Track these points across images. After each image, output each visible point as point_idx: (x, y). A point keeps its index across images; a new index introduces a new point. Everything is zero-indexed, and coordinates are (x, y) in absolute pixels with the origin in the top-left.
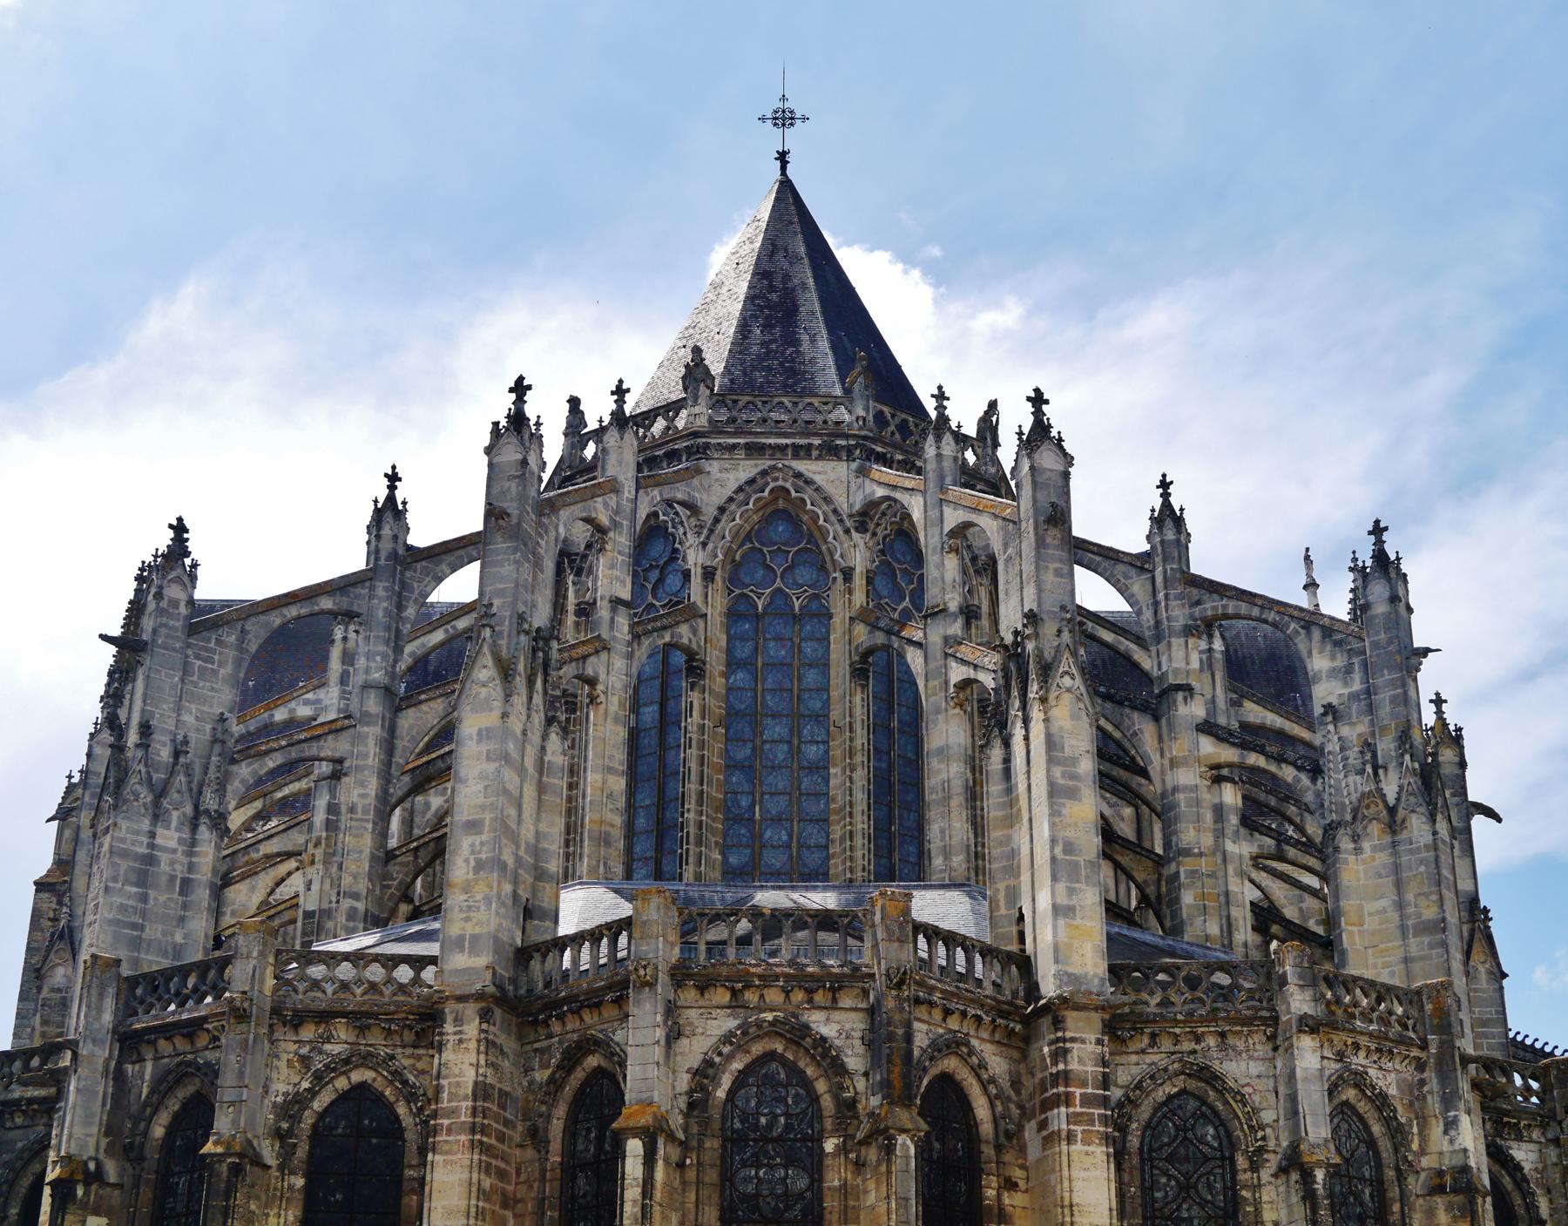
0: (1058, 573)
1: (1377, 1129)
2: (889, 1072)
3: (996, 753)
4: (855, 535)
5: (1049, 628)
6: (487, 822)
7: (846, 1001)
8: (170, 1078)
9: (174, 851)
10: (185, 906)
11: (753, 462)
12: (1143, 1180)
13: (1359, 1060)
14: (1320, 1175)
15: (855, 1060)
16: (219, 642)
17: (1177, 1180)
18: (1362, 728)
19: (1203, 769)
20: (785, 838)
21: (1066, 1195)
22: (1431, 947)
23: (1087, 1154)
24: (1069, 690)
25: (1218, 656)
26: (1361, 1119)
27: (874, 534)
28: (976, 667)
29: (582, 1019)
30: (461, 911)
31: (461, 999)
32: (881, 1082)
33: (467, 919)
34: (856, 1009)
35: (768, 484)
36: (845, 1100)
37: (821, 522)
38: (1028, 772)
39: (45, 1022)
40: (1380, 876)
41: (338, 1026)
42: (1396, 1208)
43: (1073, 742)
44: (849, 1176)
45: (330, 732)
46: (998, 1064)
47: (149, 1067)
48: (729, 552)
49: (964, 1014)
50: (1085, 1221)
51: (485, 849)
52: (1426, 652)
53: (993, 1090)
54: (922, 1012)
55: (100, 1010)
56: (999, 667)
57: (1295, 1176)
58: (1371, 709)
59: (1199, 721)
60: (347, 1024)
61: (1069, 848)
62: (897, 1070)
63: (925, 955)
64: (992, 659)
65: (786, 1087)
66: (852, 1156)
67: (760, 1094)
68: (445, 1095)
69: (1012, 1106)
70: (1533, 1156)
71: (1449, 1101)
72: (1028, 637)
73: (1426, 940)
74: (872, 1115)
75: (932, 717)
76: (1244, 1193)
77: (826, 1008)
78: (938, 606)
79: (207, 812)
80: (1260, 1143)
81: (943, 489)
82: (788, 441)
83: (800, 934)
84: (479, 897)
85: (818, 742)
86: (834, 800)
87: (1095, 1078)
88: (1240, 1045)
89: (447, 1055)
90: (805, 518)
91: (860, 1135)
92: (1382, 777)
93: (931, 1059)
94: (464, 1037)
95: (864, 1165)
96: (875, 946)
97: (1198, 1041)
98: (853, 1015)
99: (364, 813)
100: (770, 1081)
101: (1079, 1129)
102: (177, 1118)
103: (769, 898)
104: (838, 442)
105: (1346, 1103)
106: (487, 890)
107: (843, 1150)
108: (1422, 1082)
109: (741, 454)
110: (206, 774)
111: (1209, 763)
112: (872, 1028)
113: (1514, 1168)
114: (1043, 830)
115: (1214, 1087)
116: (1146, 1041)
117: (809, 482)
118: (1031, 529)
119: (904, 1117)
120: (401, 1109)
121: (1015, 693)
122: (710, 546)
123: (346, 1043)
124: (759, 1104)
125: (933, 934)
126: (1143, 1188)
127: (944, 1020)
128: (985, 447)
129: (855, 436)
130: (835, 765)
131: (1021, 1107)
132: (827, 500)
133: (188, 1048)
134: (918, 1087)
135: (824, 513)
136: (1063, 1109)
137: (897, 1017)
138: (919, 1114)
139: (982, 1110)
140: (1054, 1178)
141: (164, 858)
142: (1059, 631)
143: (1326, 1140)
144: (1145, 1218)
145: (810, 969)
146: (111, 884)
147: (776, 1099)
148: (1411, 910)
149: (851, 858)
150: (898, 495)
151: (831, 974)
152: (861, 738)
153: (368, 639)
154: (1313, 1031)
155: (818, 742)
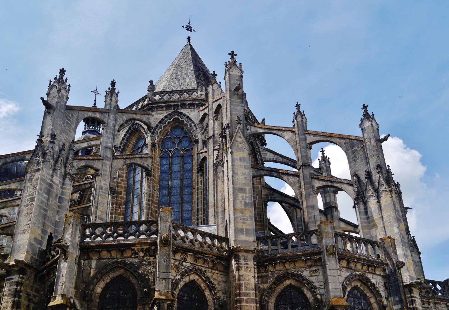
8: (108, 268)
9: (58, 185)
10: (60, 207)
16: (72, 115)
29: (284, 266)
30: (241, 219)
31: (247, 251)
33: (244, 223)
34: (380, 275)
41: (189, 256)
45: (97, 159)
47: (94, 263)
51: (247, 199)
55: (75, 236)
60: (192, 256)
67: (354, 301)
68: (243, 287)
77: (372, 273)
78: (307, 163)
79: (69, 174)
89: (242, 272)
94: (249, 266)
97: (429, 305)
99: (105, 190)
100: (355, 296)
102: (107, 285)
106: (250, 214)
110: (68, 160)
111: (344, 230)
120: (207, 293)
122: (204, 134)
123: (191, 263)
124: (354, 304)
133: (119, 256)
141: (55, 186)
146: (40, 191)
153: (107, 132)
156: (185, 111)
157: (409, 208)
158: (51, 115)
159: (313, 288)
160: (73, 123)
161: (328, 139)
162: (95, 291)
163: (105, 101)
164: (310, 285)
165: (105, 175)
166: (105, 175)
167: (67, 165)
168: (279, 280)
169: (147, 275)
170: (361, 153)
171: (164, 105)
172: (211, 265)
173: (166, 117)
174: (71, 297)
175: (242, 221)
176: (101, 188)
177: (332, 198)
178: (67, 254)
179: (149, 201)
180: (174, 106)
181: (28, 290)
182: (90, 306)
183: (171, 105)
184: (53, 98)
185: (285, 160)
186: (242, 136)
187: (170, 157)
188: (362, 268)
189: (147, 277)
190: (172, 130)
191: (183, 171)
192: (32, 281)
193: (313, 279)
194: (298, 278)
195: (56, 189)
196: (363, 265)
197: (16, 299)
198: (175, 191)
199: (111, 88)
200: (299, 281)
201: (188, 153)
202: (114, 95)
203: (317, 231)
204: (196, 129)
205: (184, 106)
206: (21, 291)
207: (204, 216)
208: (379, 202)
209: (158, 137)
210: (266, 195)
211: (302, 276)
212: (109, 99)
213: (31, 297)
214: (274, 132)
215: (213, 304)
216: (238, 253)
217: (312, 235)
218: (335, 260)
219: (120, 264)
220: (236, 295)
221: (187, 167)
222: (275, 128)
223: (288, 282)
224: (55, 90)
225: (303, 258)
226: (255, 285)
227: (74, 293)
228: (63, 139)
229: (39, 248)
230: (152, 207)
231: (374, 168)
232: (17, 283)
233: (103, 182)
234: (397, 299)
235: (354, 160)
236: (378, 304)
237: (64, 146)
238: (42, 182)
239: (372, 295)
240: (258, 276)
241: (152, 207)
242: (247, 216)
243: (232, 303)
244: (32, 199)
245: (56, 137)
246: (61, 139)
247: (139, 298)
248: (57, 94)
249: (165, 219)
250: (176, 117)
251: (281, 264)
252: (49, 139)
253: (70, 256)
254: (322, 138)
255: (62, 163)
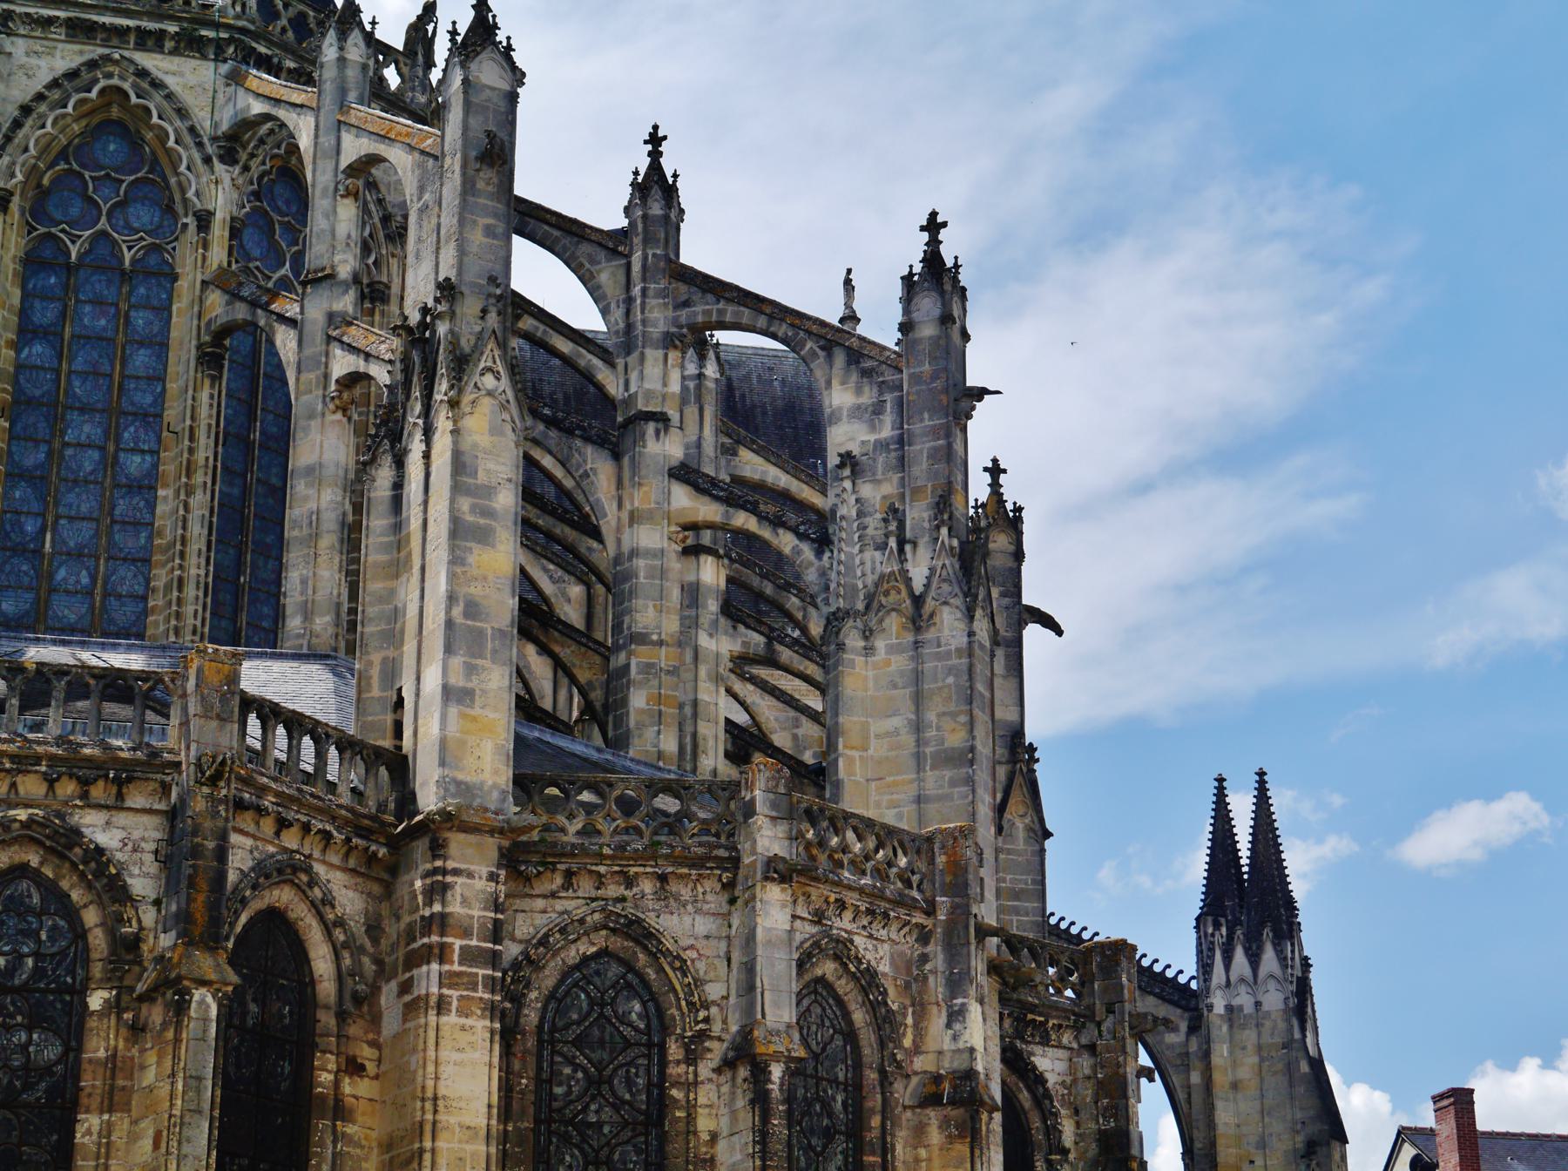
0: (489, 231)
1: (859, 1017)
2: (190, 900)
3: (384, 475)
4: (219, 167)
5: (470, 307)
7: (136, 799)
11: (77, 47)
12: (539, 1068)
13: (843, 924)
14: (777, 1071)
15: (142, 882)
17: (585, 1071)
18: (889, 488)
19: (674, 528)
20: (85, 580)
21: (430, 1083)
22: (953, 783)
23: (463, 1028)
24: (490, 394)
25: (711, 385)
26: (840, 1002)
27: (246, 168)
28: (368, 356)
32: (177, 915)
34: (150, 811)
35: (96, 81)
36: (124, 937)
37: (171, 143)
38: (426, 503)
40: (895, 687)
42: (876, 1121)
43: (491, 466)
44: (121, 1044)
46: (349, 900)
48: (33, 172)
49: (306, 828)
50: (452, 1120)
52: (981, 393)
53: (340, 936)
54: (246, 821)
56: (397, 357)
57: (743, 1072)
58: (902, 464)
59: (674, 463)
61: (472, 609)
62: (201, 898)
63: (258, 746)
64: (389, 346)
65: (39, 915)
66: (128, 1016)
69: (366, 960)
70: (1061, 1066)
71: (956, 984)
72: (440, 316)
73: (948, 774)
74: (160, 959)
75: (302, 423)
76: (674, 1092)
77: (107, 807)
78: (323, 269)
80: (701, 1026)
81: (343, 107)
82: (131, 23)
83: (80, 704)
85: (143, 452)
86: (160, 534)
87: (482, 926)
90: (149, 136)
91: (141, 988)
92: (909, 556)
93: (254, 887)
95: (143, 1030)
96: (185, 724)
98: (145, 819)
101: (454, 994)
103: (38, 653)
104: (204, 33)
105: (821, 980)
107: (114, 1007)
108: (924, 958)
109: (59, 33)
111: (682, 521)
112: (171, 840)
113: (1035, 1080)
114: (439, 583)
115: (645, 948)
116: (559, 880)
117: (157, 85)
118: (457, 168)
119: (205, 963)
121: (416, 393)
125: (270, 713)
126: (538, 1080)
127: (277, 834)
128: (414, 65)
129: (228, 27)
130: (165, 486)
131: (378, 962)
132: (182, 113)
134: (232, 925)
135: (176, 130)
136: (435, 966)
137: (208, 824)
138: (231, 962)
139: (322, 963)
140: (414, 1060)
142: (484, 311)
143: (789, 1026)
144: (537, 1121)
145: (87, 751)
147: (22, 932)
148: (931, 733)
149: (178, 616)
150: (282, 113)
151: (117, 760)
152: (205, 449)
154: (784, 879)
155: (143, 452)
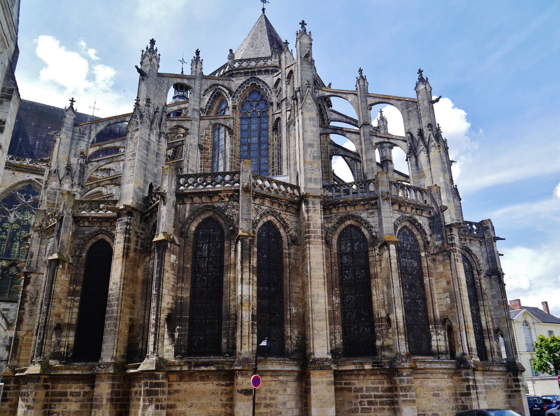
6: (315, 145)
8: (200, 211)
9: (154, 143)
10: (157, 161)
16: (163, 82)
29: (346, 209)
31: (315, 197)
33: (312, 173)
39: (48, 199)
41: (266, 200)
47: (188, 207)
51: (316, 153)
55: (171, 183)
60: (269, 200)
67: (403, 237)
77: (419, 215)
79: (163, 132)
84: (315, 167)
88: (474, 244)
89: (310, 214)
97: (465, 241)
99: (195, 147)
100: (404, 234)
102: (200, 224)
106: (318, 166)
120: (282, 231)
124: (403, 240)
133: (208, 201)
141: (152, 144)
153: (194, 96)
156: (261, 77)
157: (454, 162)
158: (145, 82)
159: (369, 227)
160: (164, 89)
161: (387, 101)
162: (190, 229)
163: (191, 69)
164: (367, 225)
165: (194, 134)
166: (194, 134)
167: (162, 125)
168: (342, 220)
169: (232, 217)
170: (415, 113)
171: (242, 71)
172: (284, 208)
173: (245, 82)
174: (171, 234)
175: (310, 172)
176: (191, 145)
177: (388, 152)
178: (165, 200)
179: (232, 155)
180: (251, 72)
181: (136, 229)
182: (186, 241)
183: (248, 71)
184: (146, 66)
185: (348, 120)
186: (311, 98)
187: (248, 118)
188: (412, 210)
189: (232, 218)
190: (250, 94)
191: (260, 129)
192: (139, 221)
193: (370, 220)
194: (357, 219)
195: (153, 146)
196: (412, 208)
197: (127, 236)
198: (254, 147)
199: (196, 56)
200: (358, 221)
201: (264, 114)
202: (199, 63)
203: (374, 180)
204: (271, 93)
205: (260, 72)
206: (130, 230)
207: (278, 168)
208: (428, 156)
209: (238, 100)
210: (332, 150)
211: (360, 217)
212: (194, 66)
213: (138, 235)
214: (339, 95)
215: (286, 240)
216: (307, 198)
217: (370, 184)
218: (388, 204)
219: (209, 207)
220: (305, 233)
221: (264, 126)
222: (340, 91)
223: (348, 222)
224: (147, 59)
225: (362, 203)
226: (322, 224)
227: (173, 231)
228: (157, 103)
229: (143, 195)
230: (235, 161)
231: (425, 126)
232: (127, 224)
233: (192, 140)
234: (439, 236)
235: (409, 119)
236: (423, 240)
237: (158, 108)
238: (141, 140)
239: (418, 233)
240: (324, 217)
241: (235, 161)
242: (315, 167)
243: (302, 239)
244: (134, 155)
245: (150, 101)
246: (155, 103)
247: (226, 235)
248: (149, 62)
249: (245, 170)
250: (254, 82)
251: (343, 207)
252: (145, 103)
253: (168, 202)
254: (381, 100)
255: (157, 123)
